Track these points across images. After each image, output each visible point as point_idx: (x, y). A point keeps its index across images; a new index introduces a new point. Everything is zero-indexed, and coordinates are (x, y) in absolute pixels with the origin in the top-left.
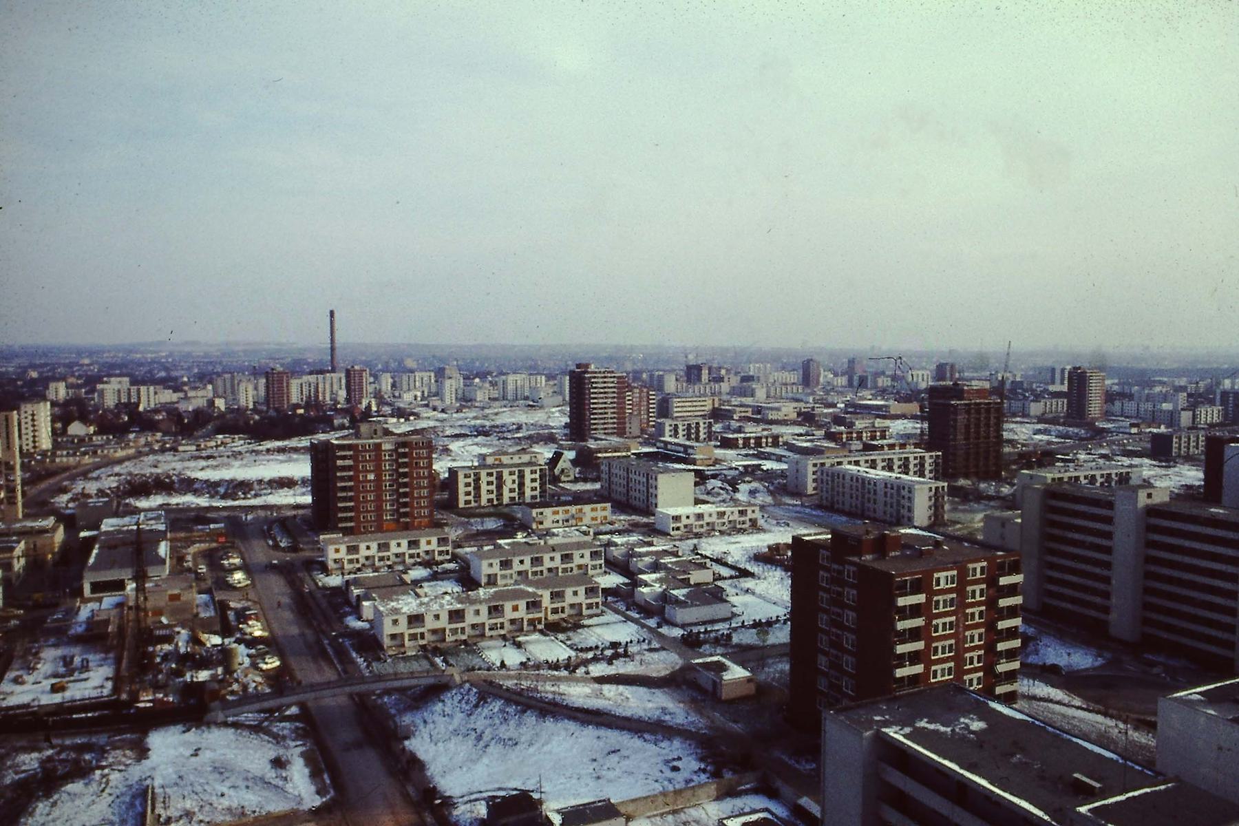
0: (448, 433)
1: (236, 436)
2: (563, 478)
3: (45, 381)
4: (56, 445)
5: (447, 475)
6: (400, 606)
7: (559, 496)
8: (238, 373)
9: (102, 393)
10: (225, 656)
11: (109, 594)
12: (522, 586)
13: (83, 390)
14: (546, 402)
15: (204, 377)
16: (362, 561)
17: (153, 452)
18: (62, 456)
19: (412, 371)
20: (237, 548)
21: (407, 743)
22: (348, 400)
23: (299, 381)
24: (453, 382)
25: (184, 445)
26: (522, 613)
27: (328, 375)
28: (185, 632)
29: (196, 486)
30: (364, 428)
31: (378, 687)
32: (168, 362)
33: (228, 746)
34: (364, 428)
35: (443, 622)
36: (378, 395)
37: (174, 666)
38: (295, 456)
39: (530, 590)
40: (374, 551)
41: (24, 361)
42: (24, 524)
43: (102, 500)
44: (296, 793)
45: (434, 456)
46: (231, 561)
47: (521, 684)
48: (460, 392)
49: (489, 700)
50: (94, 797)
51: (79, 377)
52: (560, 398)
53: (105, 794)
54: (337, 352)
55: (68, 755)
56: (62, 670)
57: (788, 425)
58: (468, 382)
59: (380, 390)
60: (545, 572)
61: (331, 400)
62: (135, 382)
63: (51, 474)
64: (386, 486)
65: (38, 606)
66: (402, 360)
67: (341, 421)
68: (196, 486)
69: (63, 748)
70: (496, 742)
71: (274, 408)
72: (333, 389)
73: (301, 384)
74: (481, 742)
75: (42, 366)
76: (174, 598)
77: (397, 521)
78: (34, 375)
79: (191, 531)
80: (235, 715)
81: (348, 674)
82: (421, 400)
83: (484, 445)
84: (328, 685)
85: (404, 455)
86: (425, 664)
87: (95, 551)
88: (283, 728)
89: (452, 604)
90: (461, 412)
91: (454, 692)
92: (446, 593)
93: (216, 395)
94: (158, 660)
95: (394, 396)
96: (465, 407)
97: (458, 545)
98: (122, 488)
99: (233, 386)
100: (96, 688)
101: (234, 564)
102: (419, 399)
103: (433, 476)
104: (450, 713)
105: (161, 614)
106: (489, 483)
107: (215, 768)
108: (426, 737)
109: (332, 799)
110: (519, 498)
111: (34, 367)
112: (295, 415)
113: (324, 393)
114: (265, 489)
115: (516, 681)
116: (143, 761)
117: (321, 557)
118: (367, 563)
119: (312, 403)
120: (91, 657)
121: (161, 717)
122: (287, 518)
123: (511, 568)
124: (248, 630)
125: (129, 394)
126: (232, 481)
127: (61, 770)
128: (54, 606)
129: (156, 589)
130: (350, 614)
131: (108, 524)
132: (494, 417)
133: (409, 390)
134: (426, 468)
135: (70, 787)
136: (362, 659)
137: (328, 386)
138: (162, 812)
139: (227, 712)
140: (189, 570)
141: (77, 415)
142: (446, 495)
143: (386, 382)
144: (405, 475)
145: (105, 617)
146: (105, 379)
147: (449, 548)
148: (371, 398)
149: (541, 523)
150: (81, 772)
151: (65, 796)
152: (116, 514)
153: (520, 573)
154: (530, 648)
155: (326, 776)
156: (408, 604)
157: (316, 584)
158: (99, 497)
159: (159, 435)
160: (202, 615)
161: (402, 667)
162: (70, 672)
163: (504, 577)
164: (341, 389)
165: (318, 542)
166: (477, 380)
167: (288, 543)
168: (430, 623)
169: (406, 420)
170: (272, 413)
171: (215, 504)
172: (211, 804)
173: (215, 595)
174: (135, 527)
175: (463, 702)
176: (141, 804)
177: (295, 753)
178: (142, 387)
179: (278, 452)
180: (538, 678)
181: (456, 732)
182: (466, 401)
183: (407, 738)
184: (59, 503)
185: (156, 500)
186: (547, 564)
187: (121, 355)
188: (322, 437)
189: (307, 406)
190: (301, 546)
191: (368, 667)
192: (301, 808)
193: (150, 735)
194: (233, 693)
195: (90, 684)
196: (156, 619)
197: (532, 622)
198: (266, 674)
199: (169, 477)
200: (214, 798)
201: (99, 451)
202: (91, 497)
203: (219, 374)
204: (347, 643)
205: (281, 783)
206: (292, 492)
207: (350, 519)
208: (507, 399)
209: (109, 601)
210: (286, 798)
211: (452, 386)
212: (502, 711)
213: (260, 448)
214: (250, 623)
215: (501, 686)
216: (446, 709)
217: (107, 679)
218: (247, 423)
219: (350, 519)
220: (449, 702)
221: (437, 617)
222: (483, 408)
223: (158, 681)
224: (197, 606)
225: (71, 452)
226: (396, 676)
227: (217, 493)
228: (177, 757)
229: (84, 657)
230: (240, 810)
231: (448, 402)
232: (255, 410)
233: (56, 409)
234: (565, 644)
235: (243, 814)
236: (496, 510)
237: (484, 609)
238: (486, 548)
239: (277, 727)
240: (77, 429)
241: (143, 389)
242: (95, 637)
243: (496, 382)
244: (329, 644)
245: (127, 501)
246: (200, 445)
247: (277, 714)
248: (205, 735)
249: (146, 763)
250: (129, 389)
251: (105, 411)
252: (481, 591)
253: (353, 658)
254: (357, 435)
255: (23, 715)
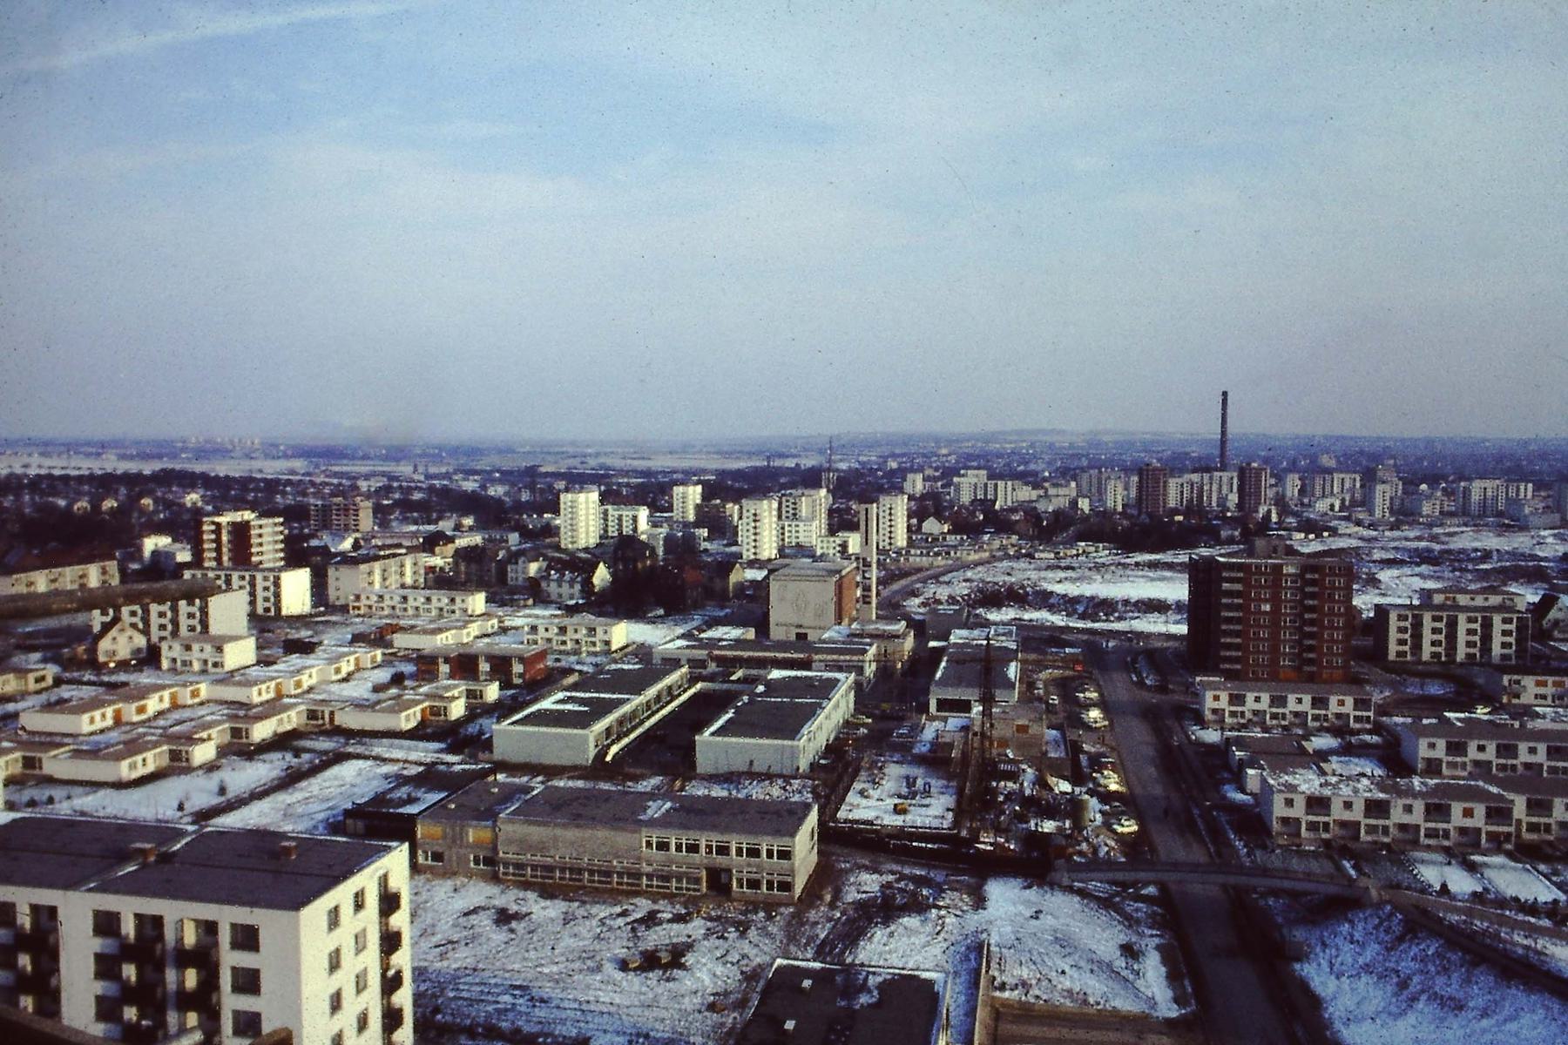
0: (1377, 555)
1: (1101, 545)
2: (1556, 634)
3: (902, 472)
4: (911, 543)
5: (1372, 614)
6: (1296, 782)
7: (1548, 658)
8: (1106, 468)
9: (958, 488)
10: (1074, 809)
11: (955, 714)
12: (1481, 783)
13: (939, 484)
14: (1534, 520)
15: (1067, 473)
16: (1248, 715)
17: (1008, 557)
18: (915, 555)
19: (1330, 471)
20: (1095, 680)
21: (1297, 966)
22: (1240, 506)
23: (1180, 481)
24: (1387, 487)
25: (1042, 551)
26: (1479, 820)
27: (1216, 473)
28: (1030, 772)
29: (1052, 601)
30: (1260, 543)
31: (1262, 883)
32: (1028, 454)
33: (1072, 916)
34: (1260, 543)
35: (1357, 814)
36: (1280, 501)
37: (1017, 808)
38: (1168, 574)
39: (1494, 790)
40: (1264, 705)
41: (886, 451)
42: (878, 626)
43: (952, 607)
44: (1150, 995)
45: (1355, 587)
46: (1088, 694)
47: (1472, 924)
48: (1397, 502)
49: (1420, 935)
50: (930, 938)
51: (936, 469)
52: (1557, 516)
53: (940, 938)
54: (1229, 446)
55: (906, 885)
56: (904, 791)
57: (632, 471)
58: (1411, 488)
59: (1284, 496)
60: (1520, 768)
61: (1218, 506)
62: (992, 476)
63: (905, 574)
64: (1285, 622)
65: (884, 717)
66: (1317, 457)
67: (1230, 532)
68: (1052, 601)
69: (902, 877)
70: (1429, 999)
71: (1147, 513)
72: (1223, 491)
73: (1182, 485)
74: (1405, 993)
75: (903, 455)
76: (1022, 729)
77: (1298, 669)
78: (893, 465)
79: (1046, 653)
80: (1082, 881)
81: (1222, 859)
82: (1340, 511)
83: (1431, 577)
84: (1195, 867)
85: (1313, 583)
86: (1328, 867)
87: (943, 664)
88: (1137, 910)
89: (1371, 791)
90: (1398, 529)
91: (1368, 912)
92: (1363, 775)
93: (1080, 494)
94: (1001, 798)
95: (1302, 504)
96: (1403, 523)
97: (1383, 710)
98: (973, 596)
99: (1100, 483)
100: (936, 817)
101: (1091, 699)
102: (1337, 508)
103: (1353, 612)
104: (1361, 939)
105: (1008, 746)
106: (1505, 633)
107: (1056, 938)
108: (1325, 964)
109: (1193, 1013)
110: (1481, 656)
111: (894, 456)
112: (1172, 522)
113: (1210, 498)
114: (1132, 612)
115: (1464, 918)
116: (980, 911)
117: (1197, 704)
118: (1255, 719)
119: (1194, 509)
120: (933, 782)
121: (1000, 866)
122: (1156, 650)
123: (1516, 757)
124: (1102, 781)
125: (986, 490)
126: (1092, 598)
127: (899, 900)
128: (900, 719)
129: (1002, 715)
130: (1229, 782)
131: (958, 636)
132: (1447, 539)
133: (1324, 496)
134: (1342, 602)
135: (905, 920)
136: (1242, 843)
137: (1215, 487)
138: (996, 974)
139: (1074, 875)
140: (1040, 699)
141: (933, 510)
142: (1368, 642)
143: (1292, 486)
144: (1312, 609)
145: (948, 740)
146: (962, 472)
147: (1371, 714)
148: (1270, 504)
149: (1518, 696)
150: (918, 906)
151: (901, 929)
152: (965, 626)
153: (1476, 763)
154: (1488, 873)
155: (1187, 982)
156: (1307, 782)
157: (1188, 737)
158: (949, 604)
159: (1015, 538)
160: (1052, 755)
161: (1295, 864)
162: (913, 795)
163: (1452, 765)
164: (1232, 491)
165: (1193, 684)
166: (1424, 487)
167: (1156, 681)
168: (1337, 812)
169: (1316, 537)
170: (1144, 518)
171: (1071, 624)
172: (1050, 981)
173: (1068, 734)
174: (985, 642)
175: (1382, 929)
176: (975, 959)
177: (1150, 942)
178: (999, 482)
179: (1149, 567)
180: (1504, 919)
181: (1367, 968)
182: (1404, 514)
183: (1299, 960)
184: (910, 606)
185: (1008, 614)
186: (1524, 756)
187: (979, 444)
188: (1204, 552)
189: (1189, 511)
190: (1171, 687)
191: (1248, 855)
192: (1155, 1014)
193: (989, 883)
194: (1081, 853)
195: (932, 811)
196: (1000, 750)
197: (1492, 837)
198: (1120, 838)
199: (1022, 587)
200: (1054, 974)
201: (952, 553)
202: (942, 603)
203: (1083, 470)
204: (1223, 818)
205: (1131, 977)
206: (1163, 618)
207: (1236, 660)
208: (1469, 515)
209: (954, 721)
210: (1137, 996)
211: (1383, 495)
212: (1437, 954)
213: (1128, 561)
214: (1106, 773)
215: (1441, 920)
216: (1355, 933)
217: (948, 810)
218: (1114, 530)
219: (1236, 660)
220: (1360, 926)
221: (1348, 805)
222: (1431, 526)
223: (999, 823)
224: (1047, 743)
225: (924, 551)
226: (1287, 874)
227: (1075, 611)
228: (1016, 915)
229: (929, 780)
230: (1081, 996)
231: (1378, 513)
232: (1123, 514)
233: (913, 503)
234: (1550, 880)
235: (1085, 1002)
236: (1444, 669)
237: (1419, 806)
238: (1425, 721)
239: (1131, 907)
240: (931, 526)
241: (1001, 484)
242: (937, 760)
243: (1453, 490)
244: (1200, 816)
245: (978, 612)
246: (1059, 553)
247: (1131, 890)
248: (1048, 895)
249: (982, 915)
250: (986, 485)
251: (960, 507)
252: (1416, 782)
253: (1229, 839)
254: (1251, 553)
255: (867, 831)
